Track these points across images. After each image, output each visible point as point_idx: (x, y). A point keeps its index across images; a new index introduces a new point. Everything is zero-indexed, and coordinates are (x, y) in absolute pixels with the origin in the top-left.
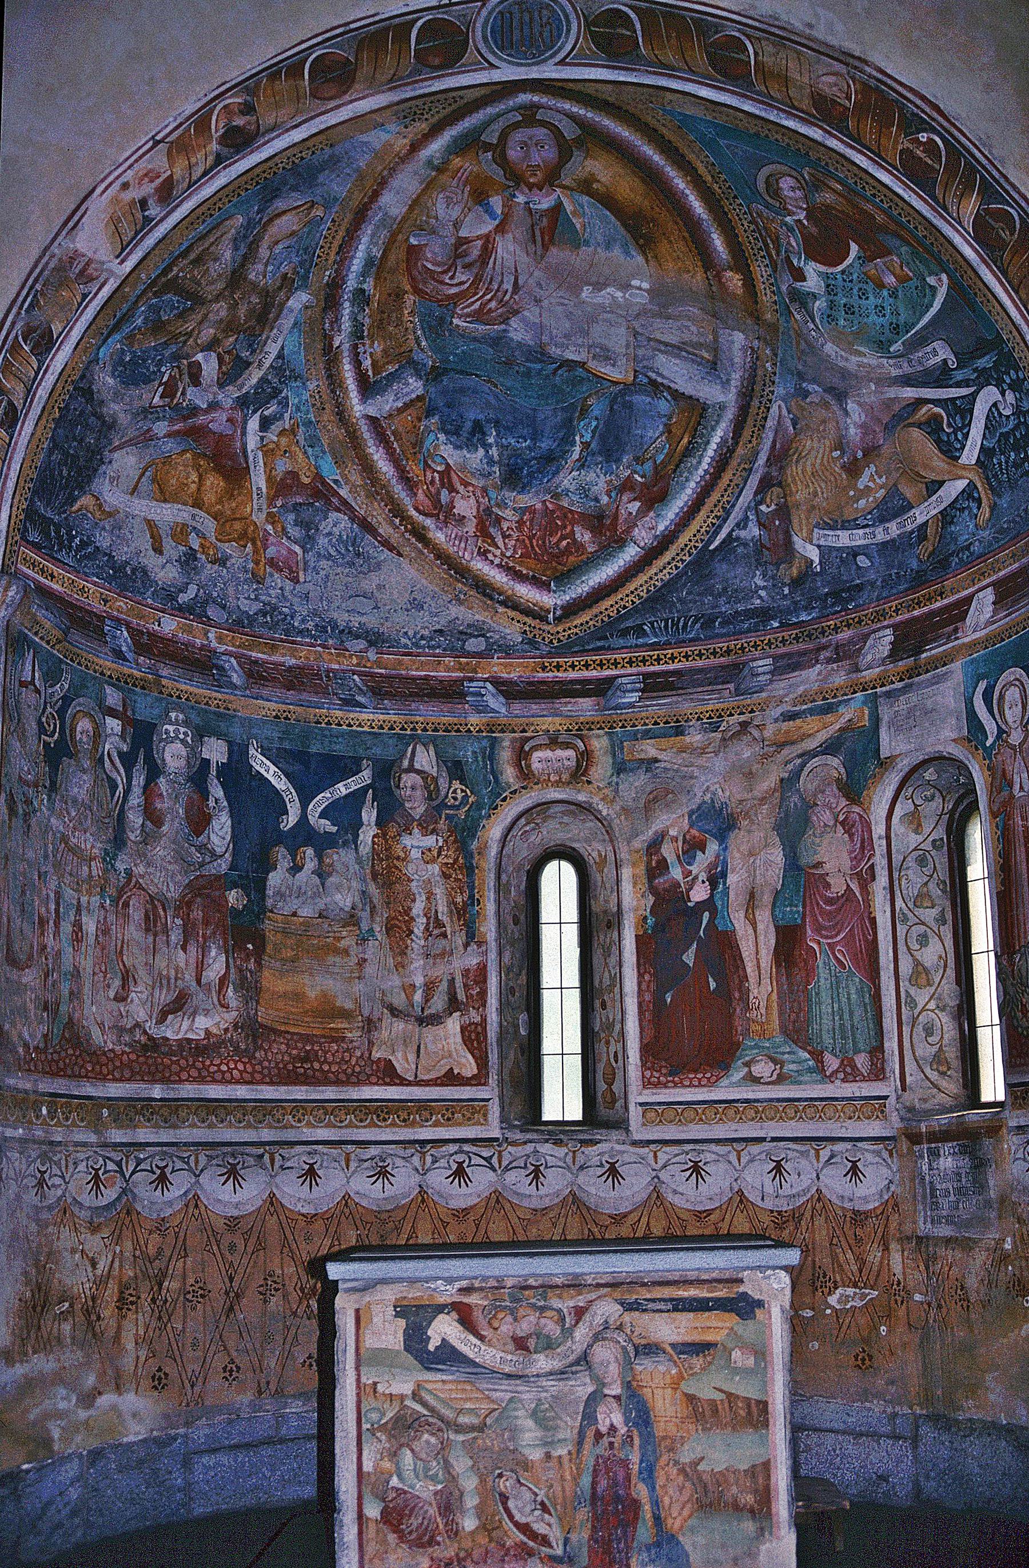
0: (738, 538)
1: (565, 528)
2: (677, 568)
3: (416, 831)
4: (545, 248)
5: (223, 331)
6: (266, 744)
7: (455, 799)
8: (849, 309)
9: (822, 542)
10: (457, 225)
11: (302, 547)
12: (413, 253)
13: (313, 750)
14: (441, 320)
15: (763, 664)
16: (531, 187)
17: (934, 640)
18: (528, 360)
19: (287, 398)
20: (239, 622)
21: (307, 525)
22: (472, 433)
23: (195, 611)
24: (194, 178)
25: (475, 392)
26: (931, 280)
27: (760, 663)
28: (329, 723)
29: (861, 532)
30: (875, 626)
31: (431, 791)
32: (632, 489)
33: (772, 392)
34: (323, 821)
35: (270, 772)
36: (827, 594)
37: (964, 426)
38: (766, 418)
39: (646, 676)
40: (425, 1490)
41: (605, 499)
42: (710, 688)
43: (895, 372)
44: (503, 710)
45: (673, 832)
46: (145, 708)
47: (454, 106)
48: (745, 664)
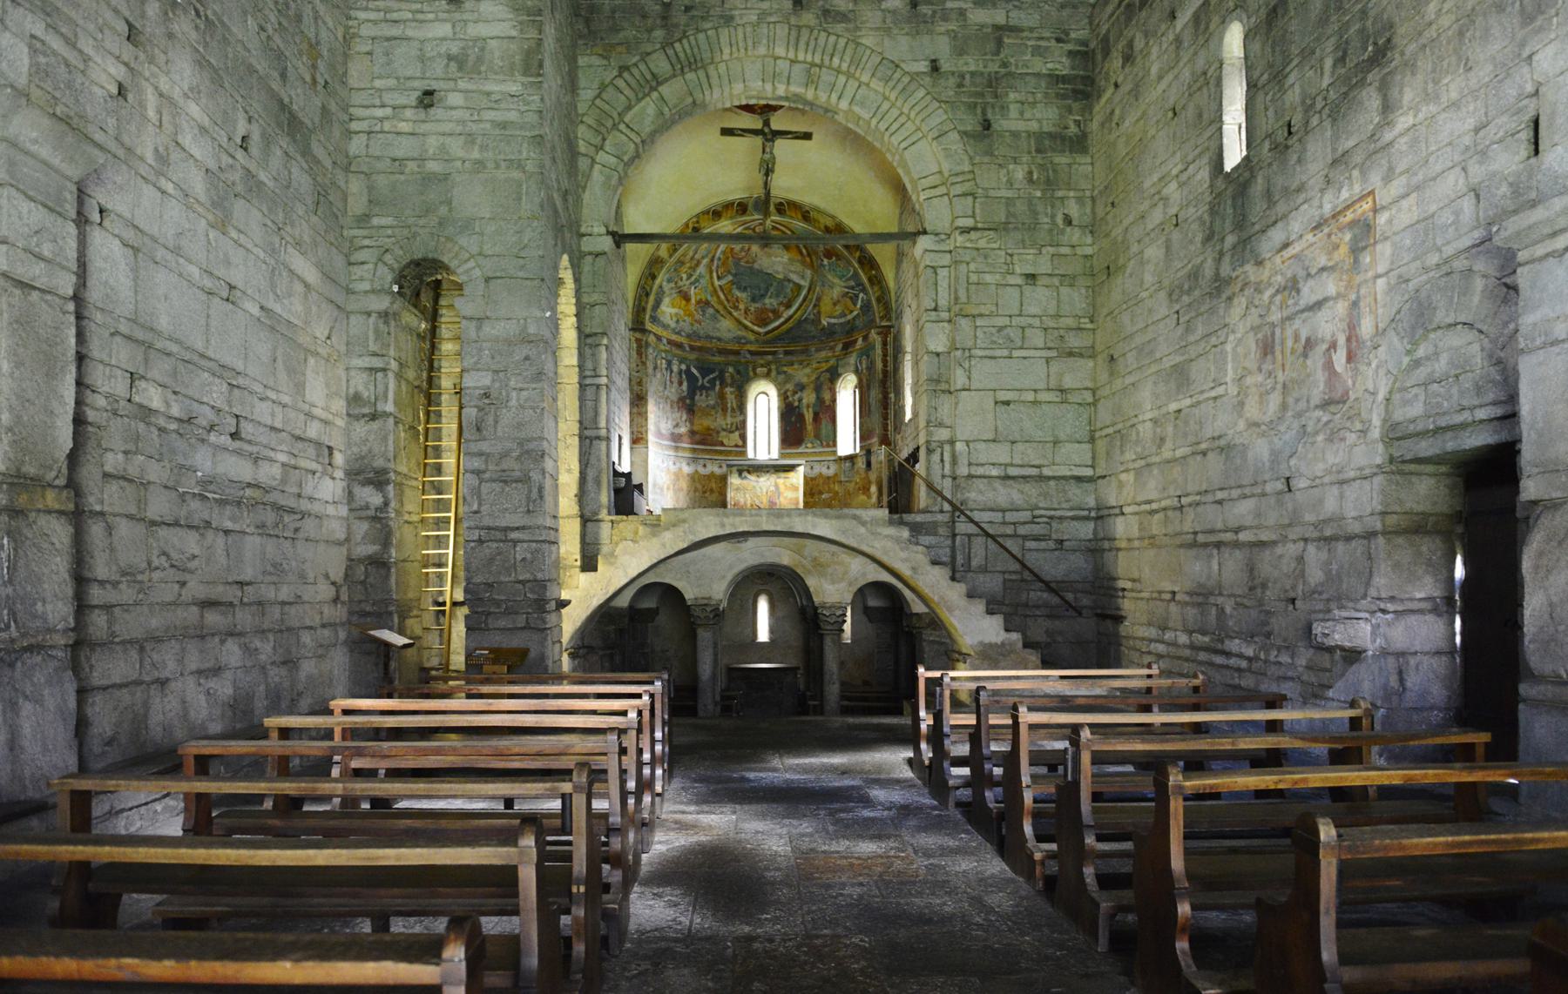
23: (678, 333)
31: (732, 377)
35: (695, 371)
40: (742, 500)
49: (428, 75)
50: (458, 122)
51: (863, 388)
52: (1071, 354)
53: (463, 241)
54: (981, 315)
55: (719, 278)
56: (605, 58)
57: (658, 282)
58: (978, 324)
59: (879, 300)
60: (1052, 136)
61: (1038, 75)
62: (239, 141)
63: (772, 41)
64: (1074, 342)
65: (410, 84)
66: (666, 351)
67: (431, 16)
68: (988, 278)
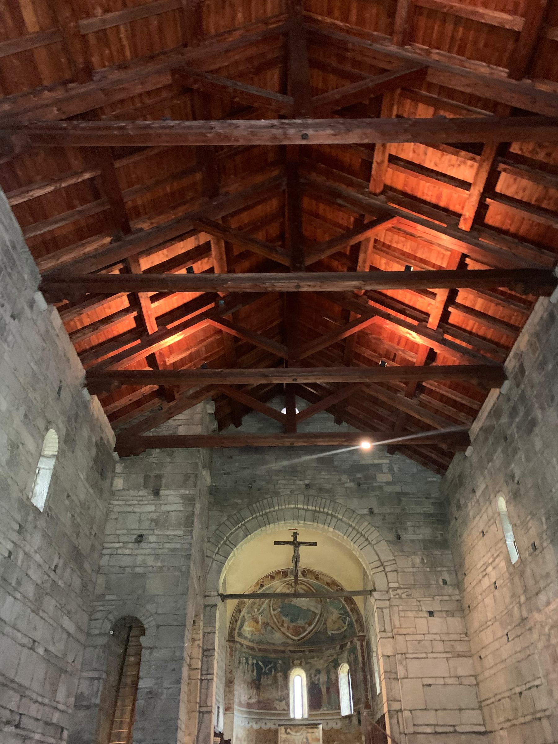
21: (266, 629)
46: (247, 656)
49: (141, 528)
50: (152, 549)
51: (352, 672)
52: (459, 656)
53: (148, 607)
54: (408, 634)
55: (274, 610)
56: (222, 512)
57: (242, 614)
58: (407, 639)
59: (356, 621)
60: (431, 541)
61: (419, 514)
62: (53, 568)
63: (297, 502)
64: (459, 648)
65: (132, 532)
66: (245, 653)
67: (146, 502)
68: (410, 614)
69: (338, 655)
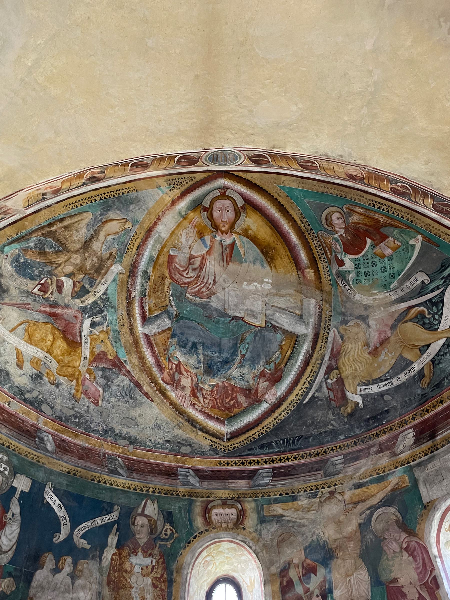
0: (317, 397)
1: (233, 395)
2: (288, 413)
3: (140, 554)
4: (228, 263)
5: (78, 271)
6: (57, 487)
7: (166, 535)
8: (367, 274)
9: (363, 393)
10: (190, 248)
11: (103, 389)
12: (171, 258)
13: (87, 495)
14: (181, 294)
15: (338, 459)
16: (223, 232)
17: (444, 428)
18: (219, 316)
19: (106, 316)
20: (59, 418)
21: (107, 379)
22: (192, 348)
24: (71, 188)
25: (194, 329)
26: (412, 242)
27: (337, 458)
28: (99, 481)
29: (384, 383)
30: (401, 430)
31: (153, 528)
32: (265, 376)
33: (330, 325)
34: (83, 541)
36: (369, 419)
37: (438, 311)
38: (327, 338)
39: (274, 469)
41: (251, 382)
42: (309, 474)
43: (394, 298)
44: (198, 485)
45: (296, 561)
47: (192, 183)
48: (328, 460)
55: (145, 320)
69: (411, 469)
